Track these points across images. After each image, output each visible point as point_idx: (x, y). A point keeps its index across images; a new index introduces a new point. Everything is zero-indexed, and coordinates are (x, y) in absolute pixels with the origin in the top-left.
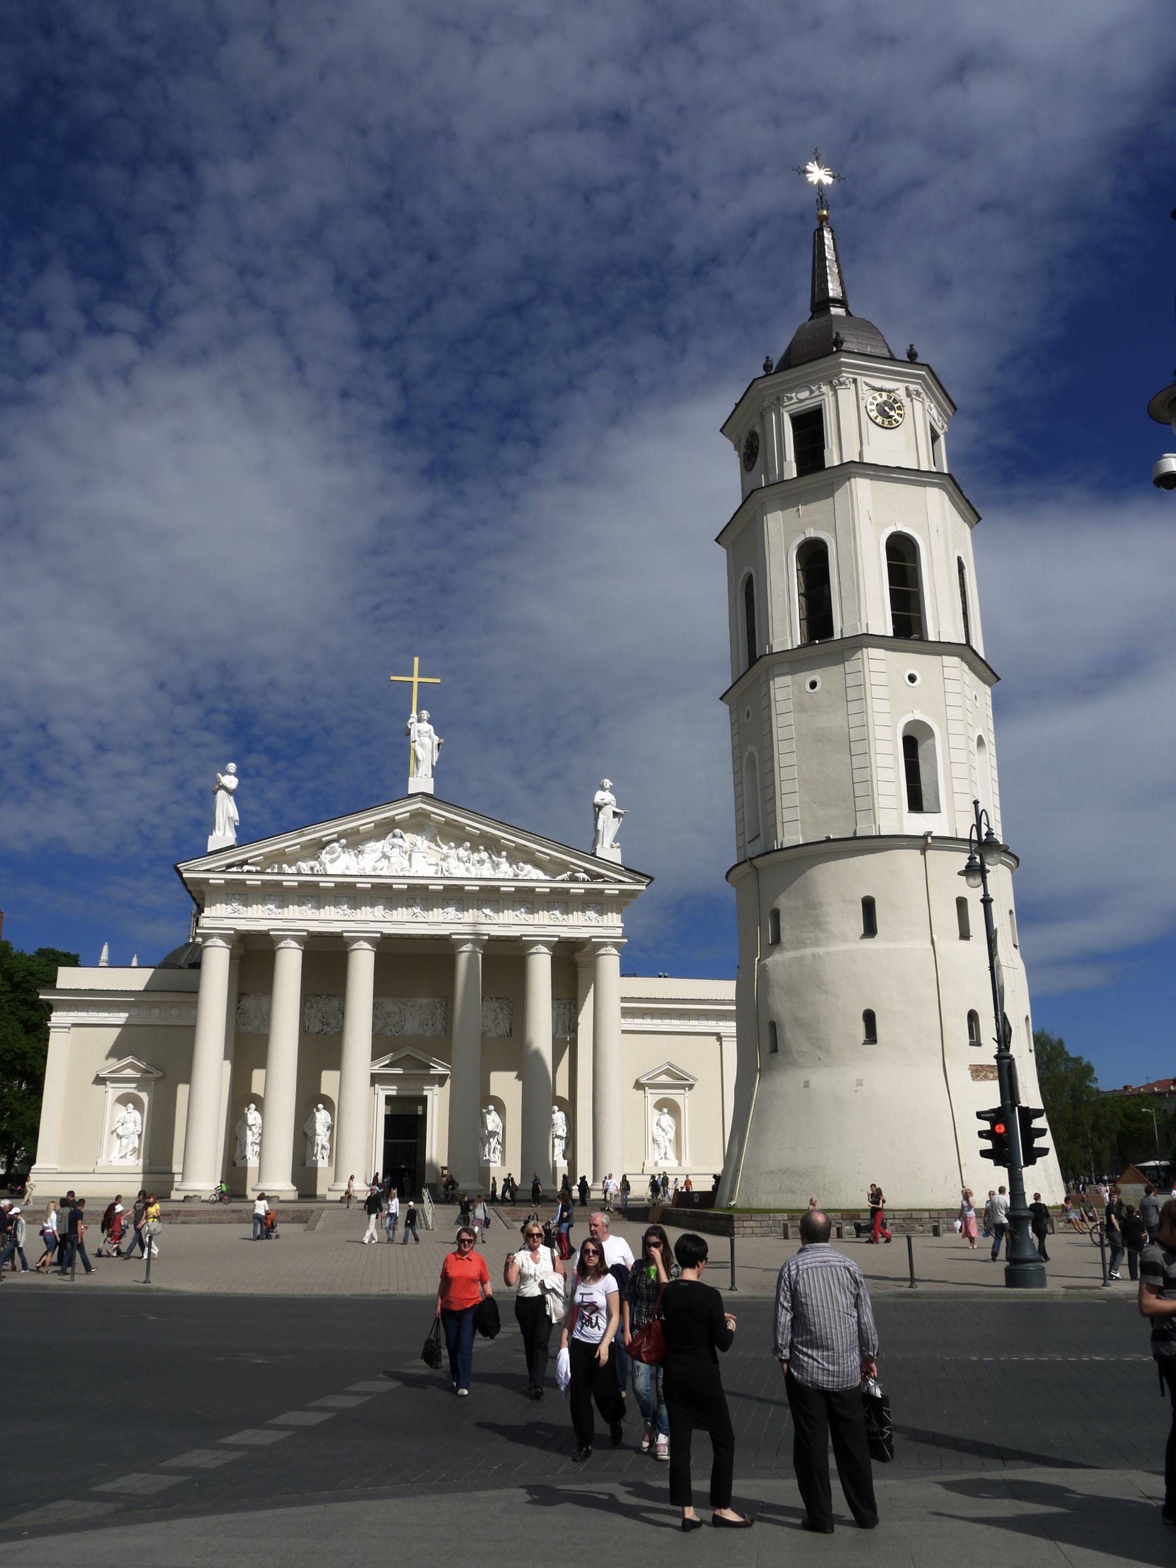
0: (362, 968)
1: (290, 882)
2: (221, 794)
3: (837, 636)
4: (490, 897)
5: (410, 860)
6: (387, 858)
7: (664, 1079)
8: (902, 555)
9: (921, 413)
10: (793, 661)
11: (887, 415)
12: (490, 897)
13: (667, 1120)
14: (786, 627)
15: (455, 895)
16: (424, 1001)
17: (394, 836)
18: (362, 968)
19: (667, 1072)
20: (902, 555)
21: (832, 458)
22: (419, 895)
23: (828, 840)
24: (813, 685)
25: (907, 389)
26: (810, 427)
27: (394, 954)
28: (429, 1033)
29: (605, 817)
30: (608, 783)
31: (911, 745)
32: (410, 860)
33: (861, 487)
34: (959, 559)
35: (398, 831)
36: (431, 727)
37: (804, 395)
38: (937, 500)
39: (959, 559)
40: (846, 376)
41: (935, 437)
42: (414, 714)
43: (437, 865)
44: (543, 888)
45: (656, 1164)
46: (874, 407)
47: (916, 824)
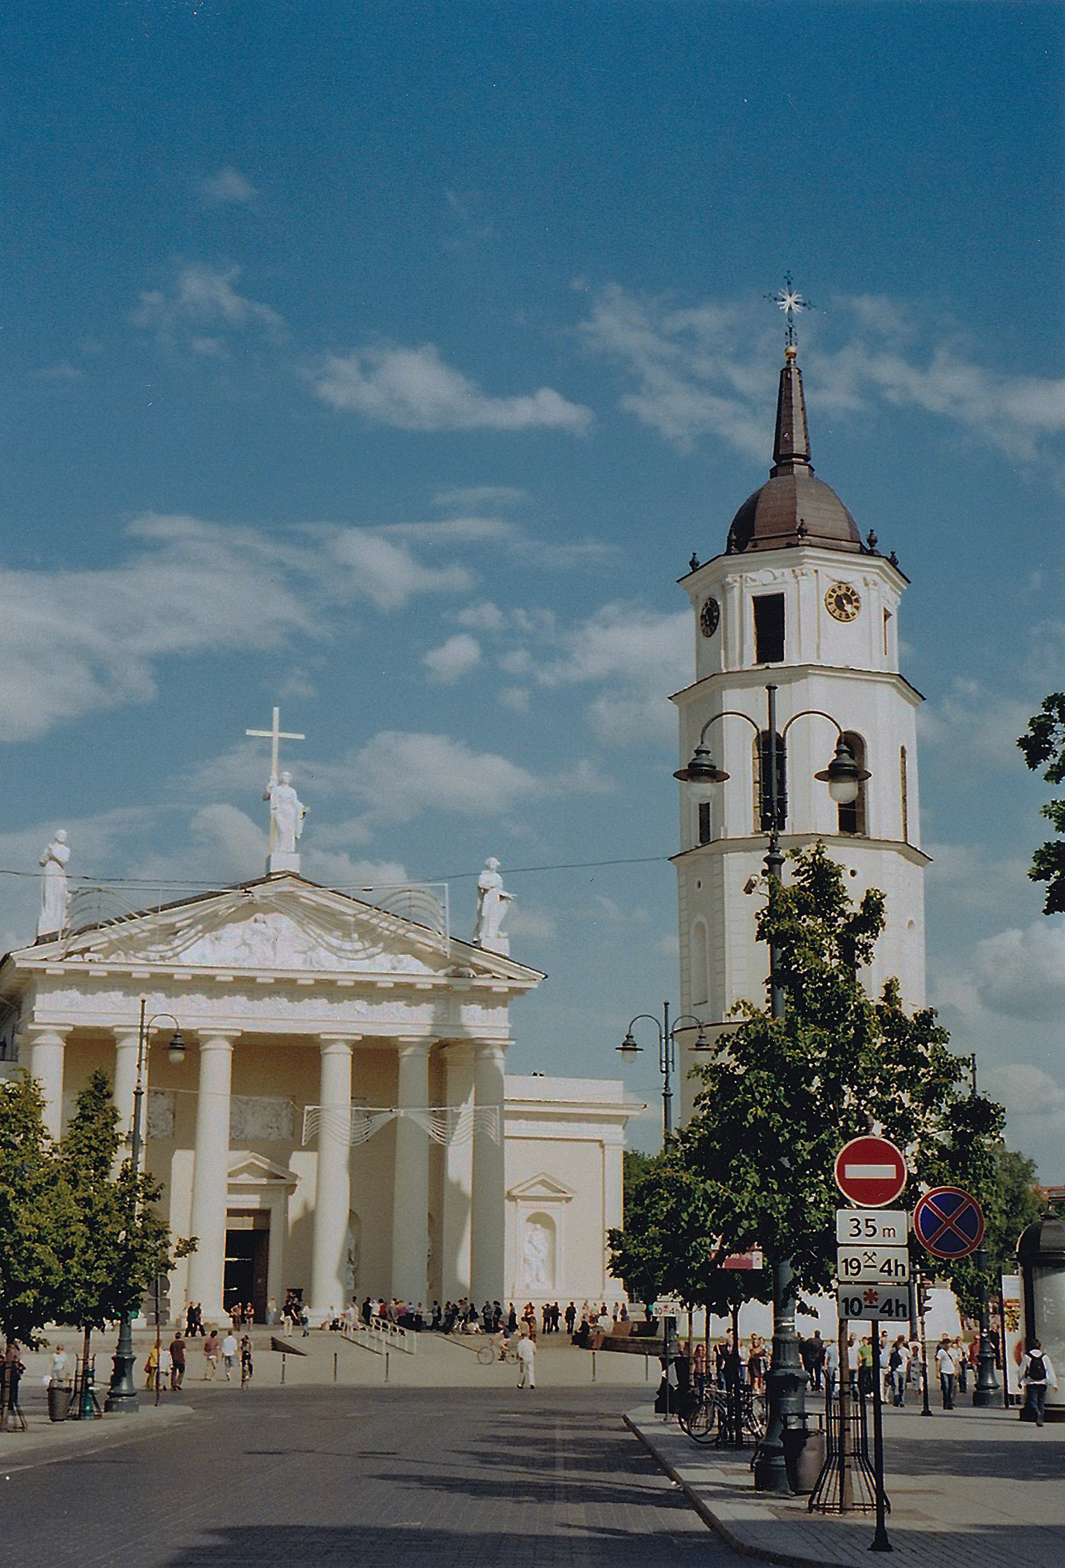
0: (217, 1067)
1: (141, 972)
2: (52, 866)
4: (366, 991)
5: (274, 947)
6: (249, 945)
7: (542, 1191)
12: (366, 991)
13: (540, 1235)
15: (328, 989)
16: (266, 1100)
17: (256, 921)
18: (217, 1067)
19: (543, 1183)
22: (288, 988)
25: (865, 579)
26: (770, 613)
27: (253, 1054)
28: (273, 1138)
29: (490, 900)
30: (494, 862)
32: (274, 947)
34: (903, 748)
35: (259, 916)
36: (294, 792)
38: (887, 695)
39: (903, 748)
40: (809, 566)
42: (274, 776)
43: (305, 953)
44: (424, 984)
45: (528, 1286)
46: (832, 600)
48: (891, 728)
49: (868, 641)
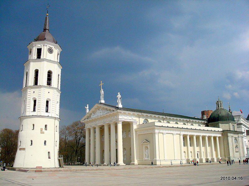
3: (38, 84)
8: (50, 74)
9: (56, 51)
10: (31, 87)
11: (50, 51)
14: (31, 82)
20: (50, 74)
21: (42, 57)
23: (33, 116)
24: (34, 92)
26: (39, 51)
31: (47, 102)
33: (45, 63)
37: (39, 45)
41: (58, 54)
47: (46, 114)
48: (57, 72)
49: (55, 56)
